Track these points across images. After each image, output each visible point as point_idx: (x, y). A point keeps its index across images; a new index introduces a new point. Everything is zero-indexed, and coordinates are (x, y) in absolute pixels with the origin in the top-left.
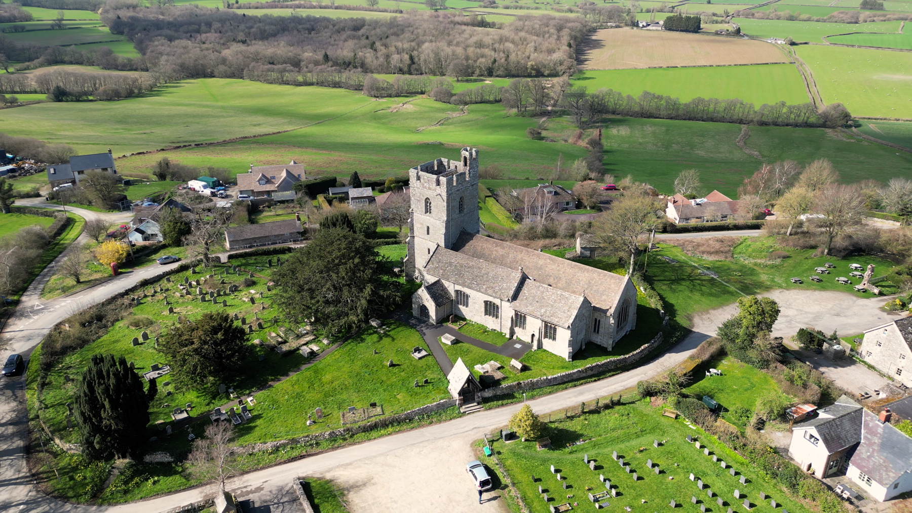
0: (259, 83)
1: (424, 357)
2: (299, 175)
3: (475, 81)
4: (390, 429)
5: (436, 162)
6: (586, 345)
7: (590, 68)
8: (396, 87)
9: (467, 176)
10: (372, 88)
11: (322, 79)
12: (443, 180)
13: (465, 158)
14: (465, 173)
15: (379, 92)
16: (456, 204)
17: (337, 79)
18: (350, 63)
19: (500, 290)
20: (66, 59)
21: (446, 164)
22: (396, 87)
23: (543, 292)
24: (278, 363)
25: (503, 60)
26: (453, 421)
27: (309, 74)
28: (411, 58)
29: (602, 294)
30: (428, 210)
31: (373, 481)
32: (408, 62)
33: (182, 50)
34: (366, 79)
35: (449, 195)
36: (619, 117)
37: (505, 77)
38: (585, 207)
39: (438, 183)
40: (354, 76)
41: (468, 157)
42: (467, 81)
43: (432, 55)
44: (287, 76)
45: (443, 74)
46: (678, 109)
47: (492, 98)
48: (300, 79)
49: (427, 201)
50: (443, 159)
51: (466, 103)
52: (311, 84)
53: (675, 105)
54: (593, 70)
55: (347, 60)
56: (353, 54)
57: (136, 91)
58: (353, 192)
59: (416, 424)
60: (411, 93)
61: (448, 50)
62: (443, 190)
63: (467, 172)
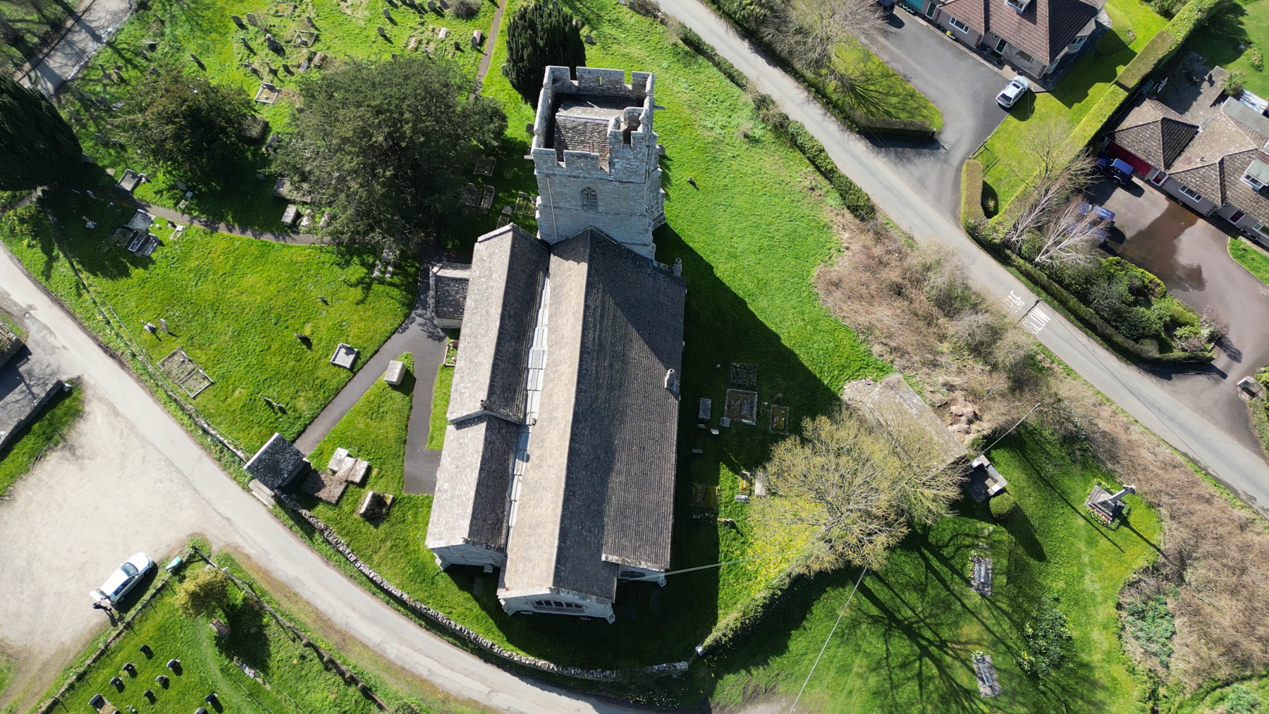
31: (86, 462)
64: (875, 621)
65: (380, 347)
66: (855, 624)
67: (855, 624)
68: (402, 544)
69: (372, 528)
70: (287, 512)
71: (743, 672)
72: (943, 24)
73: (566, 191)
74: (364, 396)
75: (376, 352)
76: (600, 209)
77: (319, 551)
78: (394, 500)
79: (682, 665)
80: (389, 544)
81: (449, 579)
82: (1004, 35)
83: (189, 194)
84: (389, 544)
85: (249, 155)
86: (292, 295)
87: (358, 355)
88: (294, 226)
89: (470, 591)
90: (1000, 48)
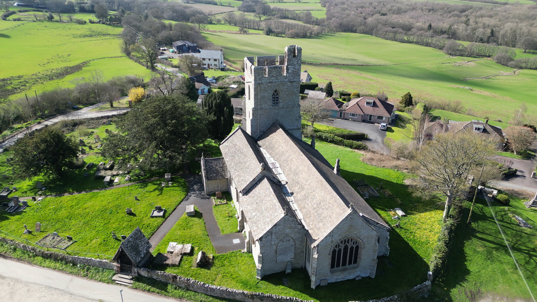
0: (380, 39)
1: (159, 217)
4: (58, 265)
6: (294, 270)
10: (450, 48)
15: (454, 52)
16: (269, 94)
17: (430, 41)
18: (445, 32)
19: (243, 180)
20: (290, 16)
22: (468, 50)
23: (265, 196)
24: (89, 180)
26: (100, 283)
28: (492, 32)
29: (321, 221)
32: (489, 34)
33: (345, 16)
34: (448, 43)
38: (513, 152)
40: (442, 40)
42: (534, 53)
43: (509, 32)
44: (398, 36)
45: (514, 46)
48: (406, 38)
51: (521, 68)
55: (444, 30)
56: (449, 26)
57: (308, 34)
59: (75, 270)
60: (480, 56)
61: (525, 30)
64: (497, 249)
65: (176, 207)
66: (490, 253)
67: (490, 253)
68: (229, 275)
69: (206, 271)
70: (144, 283)
71: (459, 286)
72: (347, 118)
73: (266, 95)
74: (177, 223)
75: (175, 209)
76: (281, 105)
77: (174, 296)
78: (213, 257)
79: (428, 283)
80: (220, 276)
81: (267, 283)
82: (370, 113)
83: (43, 189)
84: (220, 276)
85: (77, 172)
86: (118, 202)
87: (165, 211)
88: (111, 183)
89: (283, 285)
90: (370, 119)
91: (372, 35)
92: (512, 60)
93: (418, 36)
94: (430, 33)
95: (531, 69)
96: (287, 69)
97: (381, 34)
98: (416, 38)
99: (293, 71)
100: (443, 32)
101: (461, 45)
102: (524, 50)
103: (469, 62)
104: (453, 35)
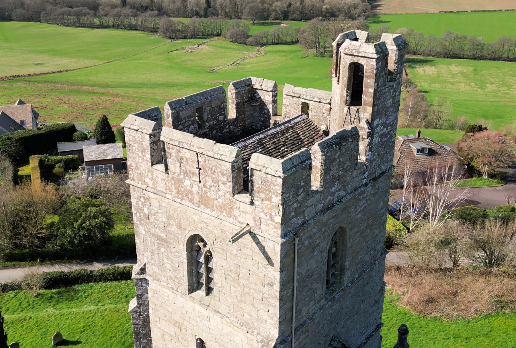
2: (23, 122)
3: (272, 24)
5: (231, 93)
7: (383, 12)
8: (191, 28)
9: (362, 146)
11: (118, 22)
12: (268, 168)
13: (356, 70)
14: (354, 134)
16: (317, 263)
17: (133, 22)
18: (147, 8)
21: (267, 98)
25: (298, 4)
27: (105, 18)
30: (199, 273)
32: (204, 5)
34: (162, 22)
35: (291, 232)
36: (421, 57)
37: (300, 20)
38: (480, 175)
39: (243, 180)
41: (369, 66)
42: (264, 24)
45: (239, 17)
46: (483, 49)
47: (289, 40)
48: (96, 21)
49: (195, 245)
50: (256, 82)
51: (262, 45)
52: (108, 27)
53: (480, 46)
54: (385, 14)
58: (92, 151)
60: (206, 35)
62: (265, 213)
63: (364, 132)
91: (39, 21)
92: (248, 37)
93: (114, 16)
94: (127, 10)
95: (273, 44)
96: (371, 135)
97: (55, 19)
98: (112, 19)
99: (381, 136)
100: (145, 9)
101: (181, 22)
102: (252, 22)
103: (199, 45)
104: (161, 12)
